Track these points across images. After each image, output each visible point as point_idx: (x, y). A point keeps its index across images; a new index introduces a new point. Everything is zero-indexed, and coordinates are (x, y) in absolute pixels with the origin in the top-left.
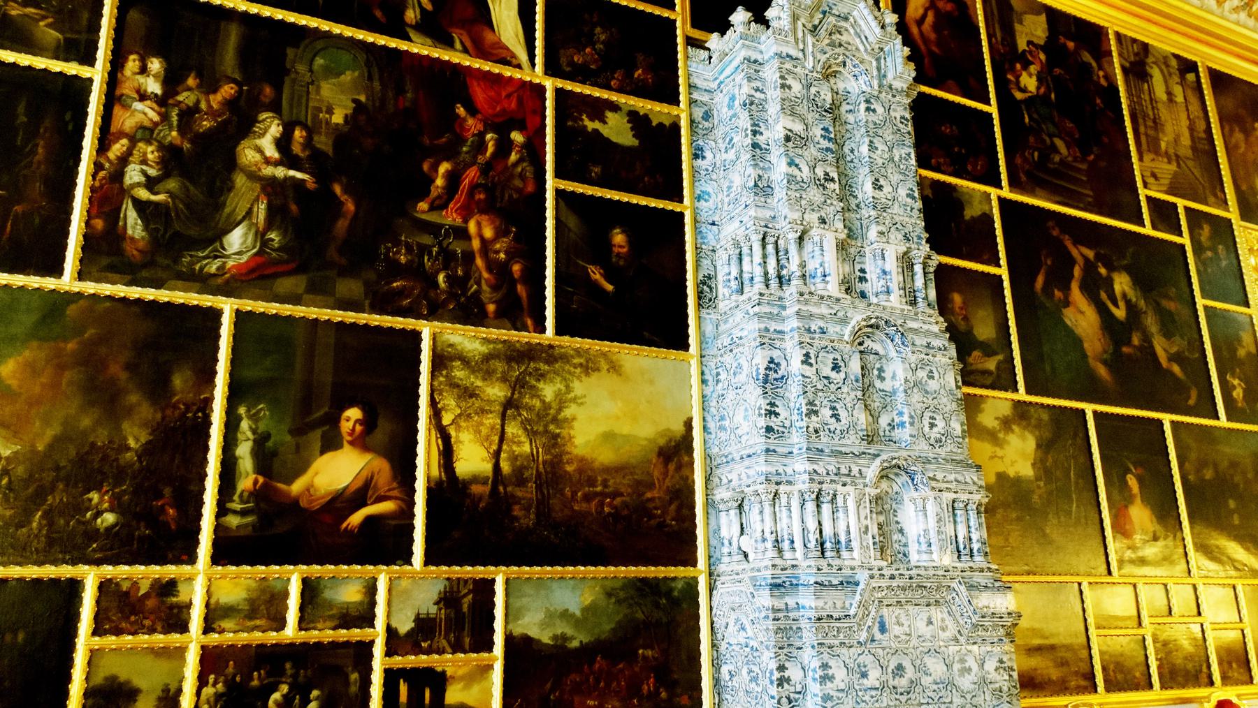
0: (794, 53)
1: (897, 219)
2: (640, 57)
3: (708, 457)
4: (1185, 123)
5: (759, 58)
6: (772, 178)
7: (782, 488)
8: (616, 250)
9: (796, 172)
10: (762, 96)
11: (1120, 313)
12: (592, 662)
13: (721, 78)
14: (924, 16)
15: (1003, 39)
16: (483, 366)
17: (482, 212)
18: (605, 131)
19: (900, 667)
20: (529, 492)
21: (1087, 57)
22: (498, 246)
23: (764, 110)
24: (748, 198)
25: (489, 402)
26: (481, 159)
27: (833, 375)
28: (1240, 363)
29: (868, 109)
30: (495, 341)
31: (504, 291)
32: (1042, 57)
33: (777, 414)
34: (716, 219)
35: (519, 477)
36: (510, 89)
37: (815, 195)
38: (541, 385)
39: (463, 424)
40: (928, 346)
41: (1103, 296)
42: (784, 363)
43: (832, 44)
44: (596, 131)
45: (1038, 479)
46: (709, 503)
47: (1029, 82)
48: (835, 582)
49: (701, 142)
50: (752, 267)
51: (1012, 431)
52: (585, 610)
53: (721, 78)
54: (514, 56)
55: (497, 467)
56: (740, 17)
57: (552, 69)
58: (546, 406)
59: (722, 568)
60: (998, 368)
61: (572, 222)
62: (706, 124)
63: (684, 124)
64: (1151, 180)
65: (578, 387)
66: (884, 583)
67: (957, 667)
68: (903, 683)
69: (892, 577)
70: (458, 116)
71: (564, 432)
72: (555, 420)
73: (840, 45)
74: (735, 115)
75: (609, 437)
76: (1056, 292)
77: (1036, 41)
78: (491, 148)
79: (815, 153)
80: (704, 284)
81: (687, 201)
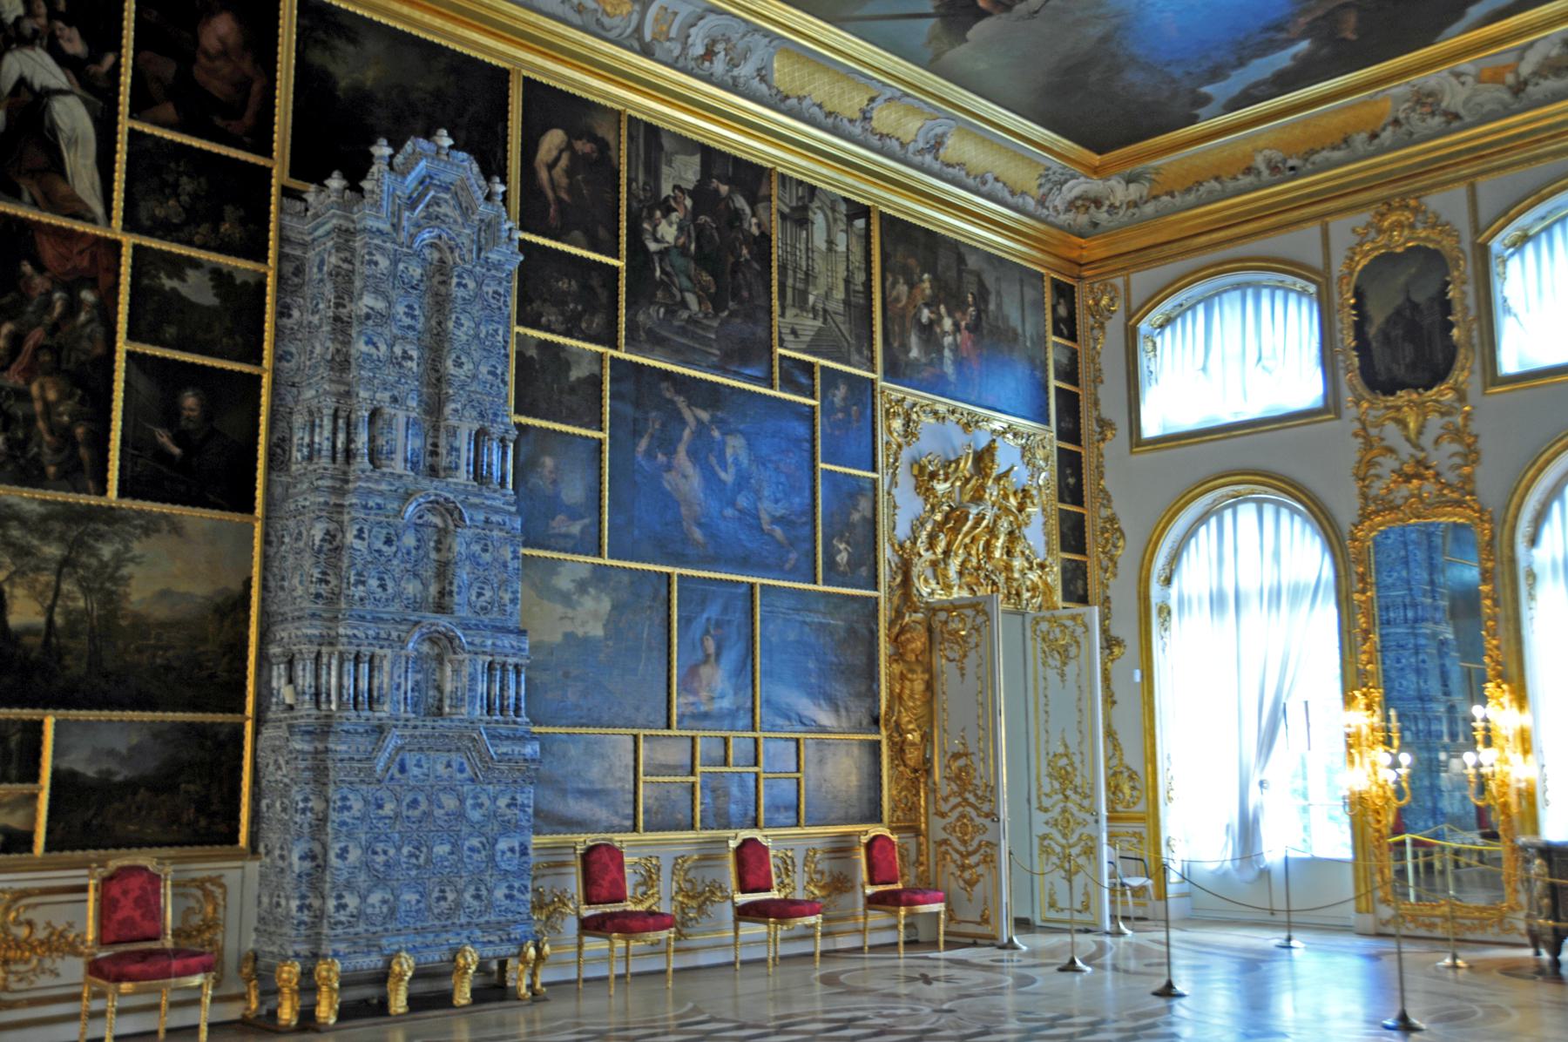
0: (386, 227)
1: (474, 396)
2: (229, 210)
3: (264, 613)
4: (842, 273)
5: (351, 226)
6: (353, 351)
7: (324, 650)
8: (186, 413)
9: (373, 350)
10: (350, 267)
11: (728, 477)
12: (135, 794)
13: (317, 234)
14: (557, 159)
15: (645, 183)
16: (41, 526)
17: (48, 374)
18: (184, 290)
19: (414, 803)
20: (82, 644)
21: (741, 202)
22: (61, 409)
23: (351, 282)
24: (323, 371)
25: (46, 560)
26: (47, 319)
27: (385, 548)
28: (850, 526)
29: (459, 284)
30: (55, 503)
31: (66, 452)
32: (688, 202)
33: (327, 582)
34: (297, 380)
35: (72, 630)
36: (82, 246)
37: (390, 374)
38: (99, 545)
39: (17, 580)
40: (487, 521)
41: (713, 460)
42: (339, 536)
43: (428, 217)
44: (173, 290)
45: (606, 638)
46: (264, 659)
47: (668, 232)
48: (361, 730)
49: (288, 300)
50: (322, 438)
51: (587, 592)
52: (132, 749)
53: (317, 234)
54: (89, 209)
55: (50, 622)
56: (335, 182)
57: (131, 224)
58: (104, 565)
59: (270, 715)
60: (583, 531)
61: (142, 383)
62: (296, 280)
63: (270, 281)
64: (791, 338)
65: (137, 548)
66: (407, 732)
67: (469, 802)
68: (416, 813)
69: (415, 727)
70: (24, 274)
71: (121, 590)
72: (112, 578)
73: (437, 217)
74: (321, 280)
75: (164, 594)
76: (660, 456)
77: (684, 185)
78: (58, 308)
79: (395, 331)
80: (278, 446)
81: (267, 362)
